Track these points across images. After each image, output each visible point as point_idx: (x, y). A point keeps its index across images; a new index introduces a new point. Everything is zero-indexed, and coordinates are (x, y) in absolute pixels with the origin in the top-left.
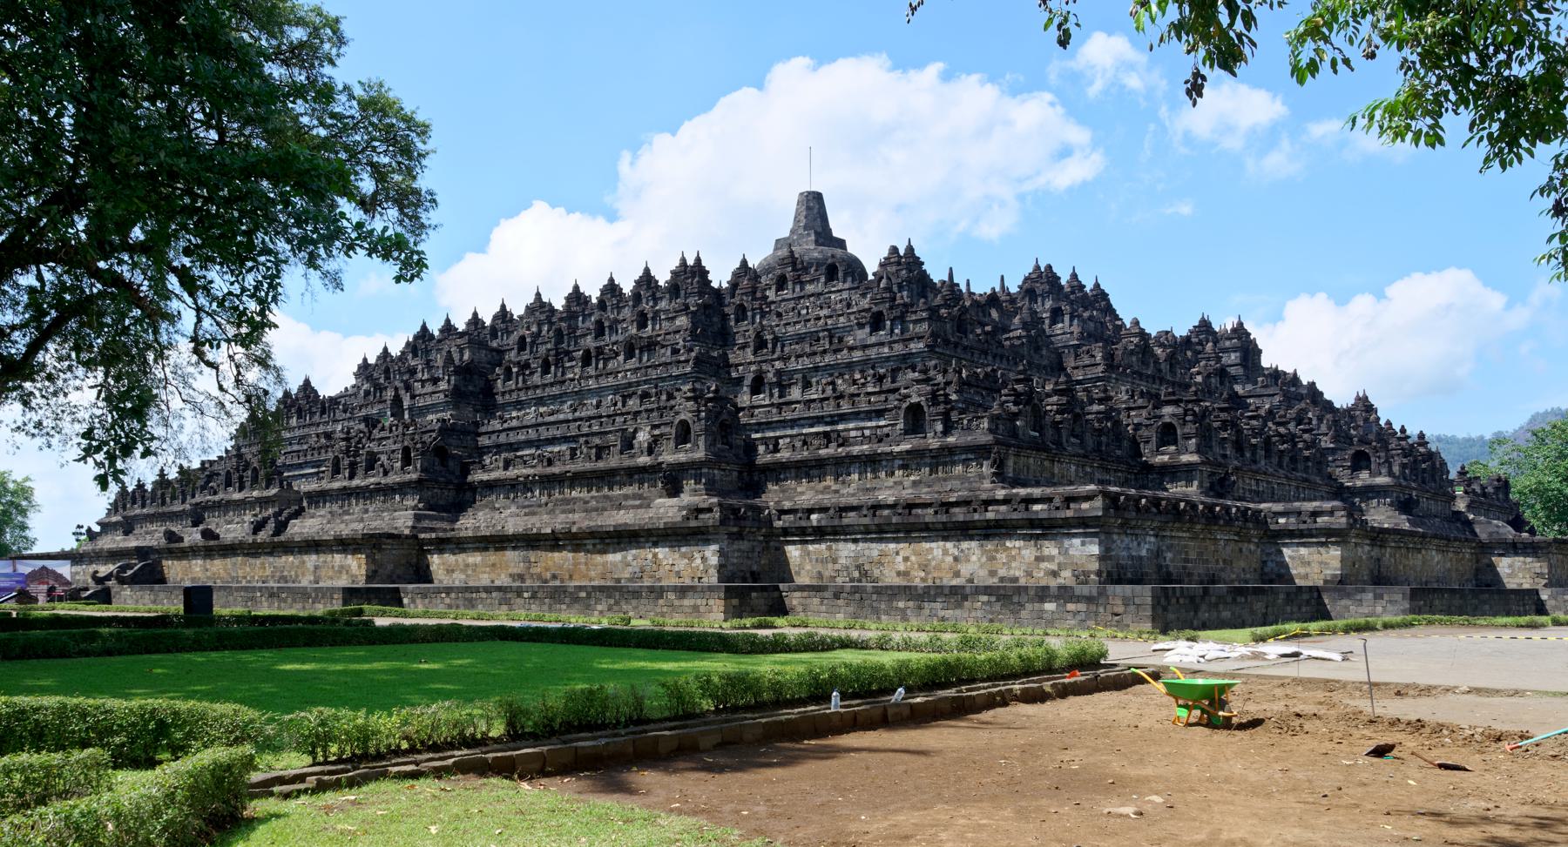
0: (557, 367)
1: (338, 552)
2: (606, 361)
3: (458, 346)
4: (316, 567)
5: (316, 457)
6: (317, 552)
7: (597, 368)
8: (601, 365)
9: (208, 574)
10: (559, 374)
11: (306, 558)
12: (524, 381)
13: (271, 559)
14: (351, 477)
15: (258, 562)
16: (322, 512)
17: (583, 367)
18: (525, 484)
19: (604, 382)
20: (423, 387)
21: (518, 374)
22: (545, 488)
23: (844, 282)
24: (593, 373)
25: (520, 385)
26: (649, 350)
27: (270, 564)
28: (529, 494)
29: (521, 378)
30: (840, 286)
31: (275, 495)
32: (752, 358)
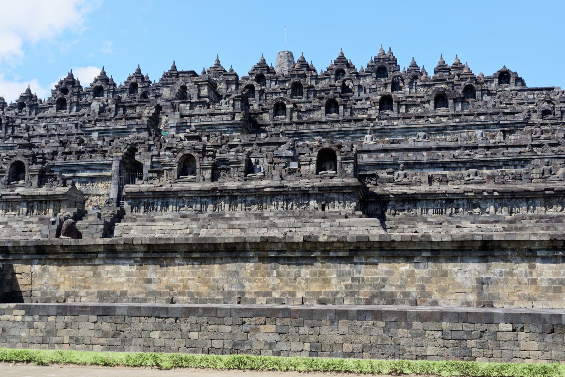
0: (345, 107)
1: (545, 259)
2: (408, 106)
3: (196, 83)
4: (482, 283)
5: (72, 160)
6: (484, 259)
7: (398, 112)
8: (403, 109)
9: (153, 287)
10: (348, 114)
11: (449, 267)
12: (299, 117)
13: (347, 268)
14: (214, 178)
15: (306, 271)
16: (165, 215)
17: (380, 109)
18: (469, 199)
19: (413, 123)
20: (191, 108)
21: (292, 110)
22: (502, 205)
23: (516, 85)
24: (396, 115)
25: (295, 119)
26: (462, 102)
27: (341, 275)
28: (477, 210)
29: (295, 115)
30: (513, 87)
31: (65, 195)
32: (540, 121)
